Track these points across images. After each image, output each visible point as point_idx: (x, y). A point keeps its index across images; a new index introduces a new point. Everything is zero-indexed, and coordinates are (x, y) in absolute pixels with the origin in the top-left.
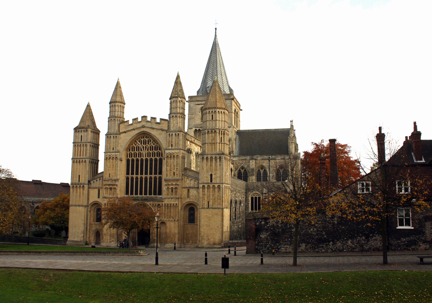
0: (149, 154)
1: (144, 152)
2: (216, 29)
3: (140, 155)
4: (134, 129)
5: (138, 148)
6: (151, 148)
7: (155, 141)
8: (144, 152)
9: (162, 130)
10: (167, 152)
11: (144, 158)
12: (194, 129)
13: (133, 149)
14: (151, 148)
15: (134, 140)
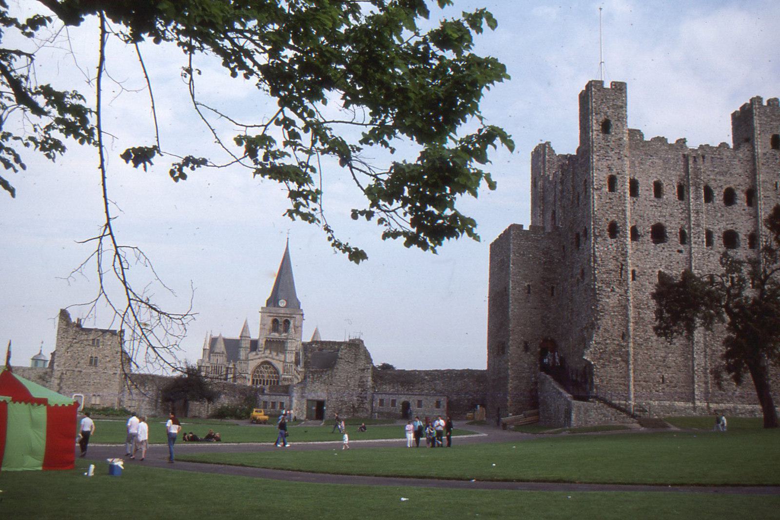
0: (269, 376)
1: (266, 375)
2: (288, 238)
3: (263, 376)
4: (259, 358)
5: (261, 372)
6: (271, 373)
7: (274, 368)
8: (266, 375)
9: (280, 361)
10: (283, 376)
11: (266, 379)
12: (265, 340)
13: (258, 372)
14: (271, 373)
15: (259, 367)
